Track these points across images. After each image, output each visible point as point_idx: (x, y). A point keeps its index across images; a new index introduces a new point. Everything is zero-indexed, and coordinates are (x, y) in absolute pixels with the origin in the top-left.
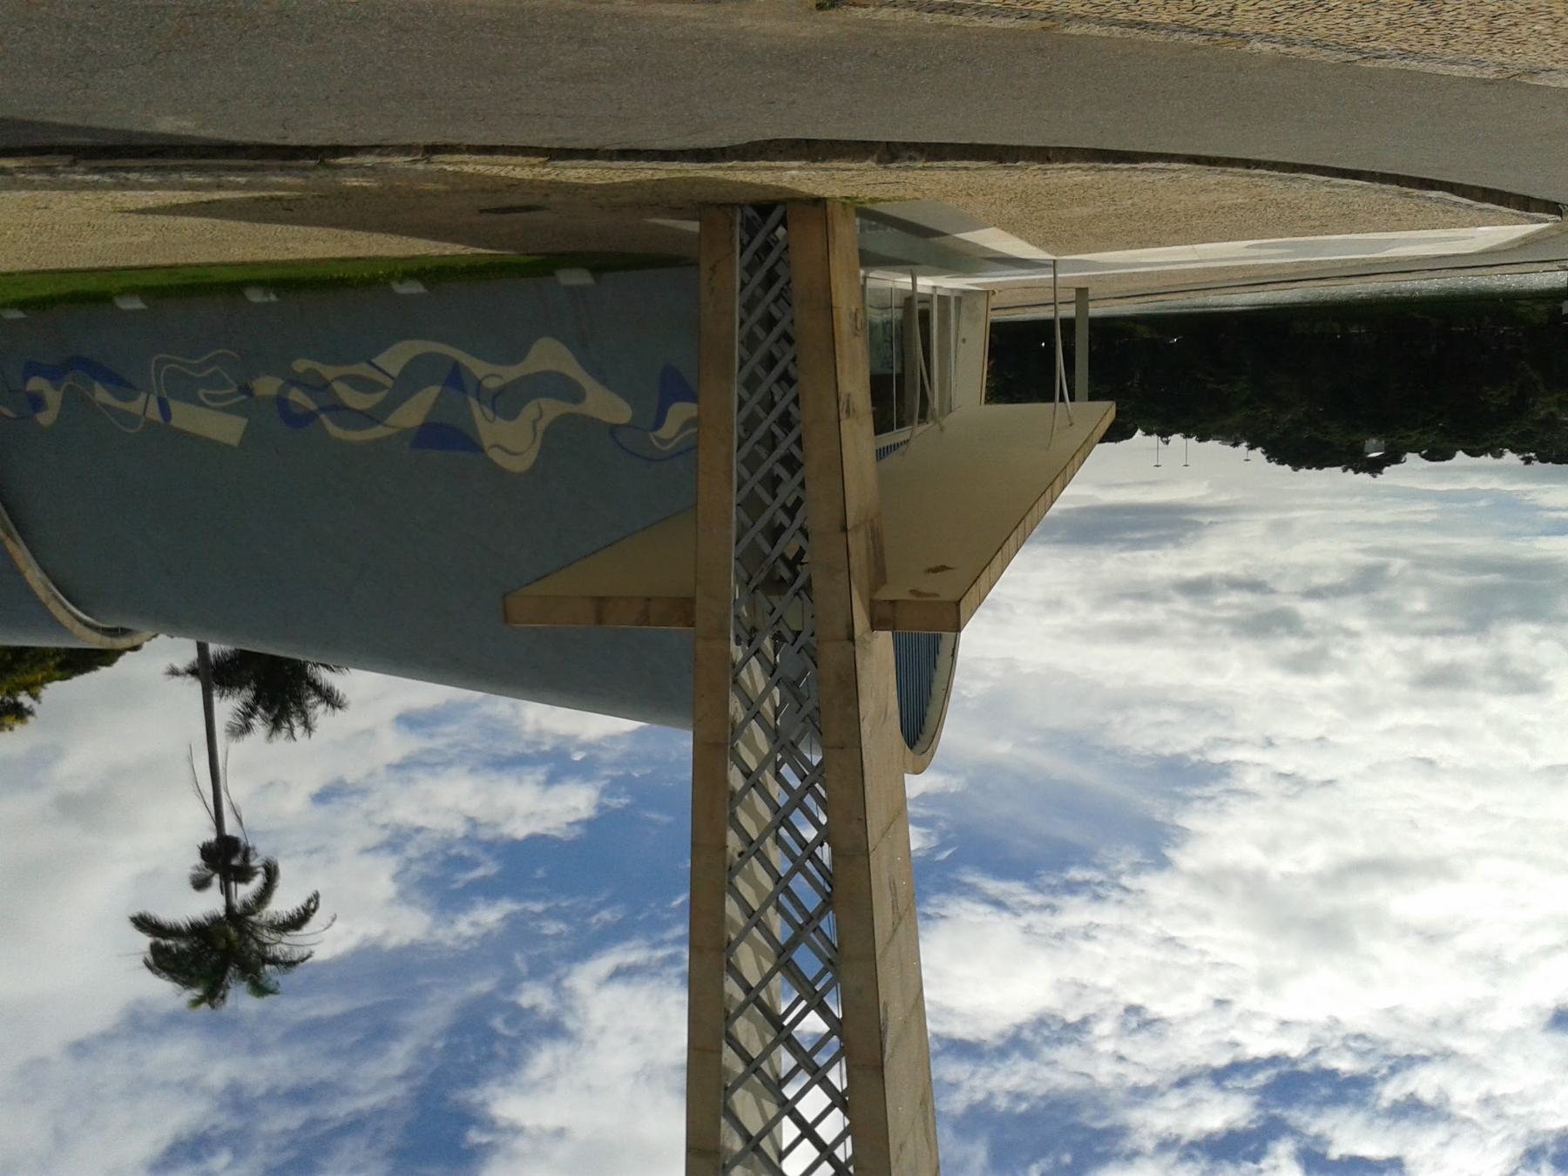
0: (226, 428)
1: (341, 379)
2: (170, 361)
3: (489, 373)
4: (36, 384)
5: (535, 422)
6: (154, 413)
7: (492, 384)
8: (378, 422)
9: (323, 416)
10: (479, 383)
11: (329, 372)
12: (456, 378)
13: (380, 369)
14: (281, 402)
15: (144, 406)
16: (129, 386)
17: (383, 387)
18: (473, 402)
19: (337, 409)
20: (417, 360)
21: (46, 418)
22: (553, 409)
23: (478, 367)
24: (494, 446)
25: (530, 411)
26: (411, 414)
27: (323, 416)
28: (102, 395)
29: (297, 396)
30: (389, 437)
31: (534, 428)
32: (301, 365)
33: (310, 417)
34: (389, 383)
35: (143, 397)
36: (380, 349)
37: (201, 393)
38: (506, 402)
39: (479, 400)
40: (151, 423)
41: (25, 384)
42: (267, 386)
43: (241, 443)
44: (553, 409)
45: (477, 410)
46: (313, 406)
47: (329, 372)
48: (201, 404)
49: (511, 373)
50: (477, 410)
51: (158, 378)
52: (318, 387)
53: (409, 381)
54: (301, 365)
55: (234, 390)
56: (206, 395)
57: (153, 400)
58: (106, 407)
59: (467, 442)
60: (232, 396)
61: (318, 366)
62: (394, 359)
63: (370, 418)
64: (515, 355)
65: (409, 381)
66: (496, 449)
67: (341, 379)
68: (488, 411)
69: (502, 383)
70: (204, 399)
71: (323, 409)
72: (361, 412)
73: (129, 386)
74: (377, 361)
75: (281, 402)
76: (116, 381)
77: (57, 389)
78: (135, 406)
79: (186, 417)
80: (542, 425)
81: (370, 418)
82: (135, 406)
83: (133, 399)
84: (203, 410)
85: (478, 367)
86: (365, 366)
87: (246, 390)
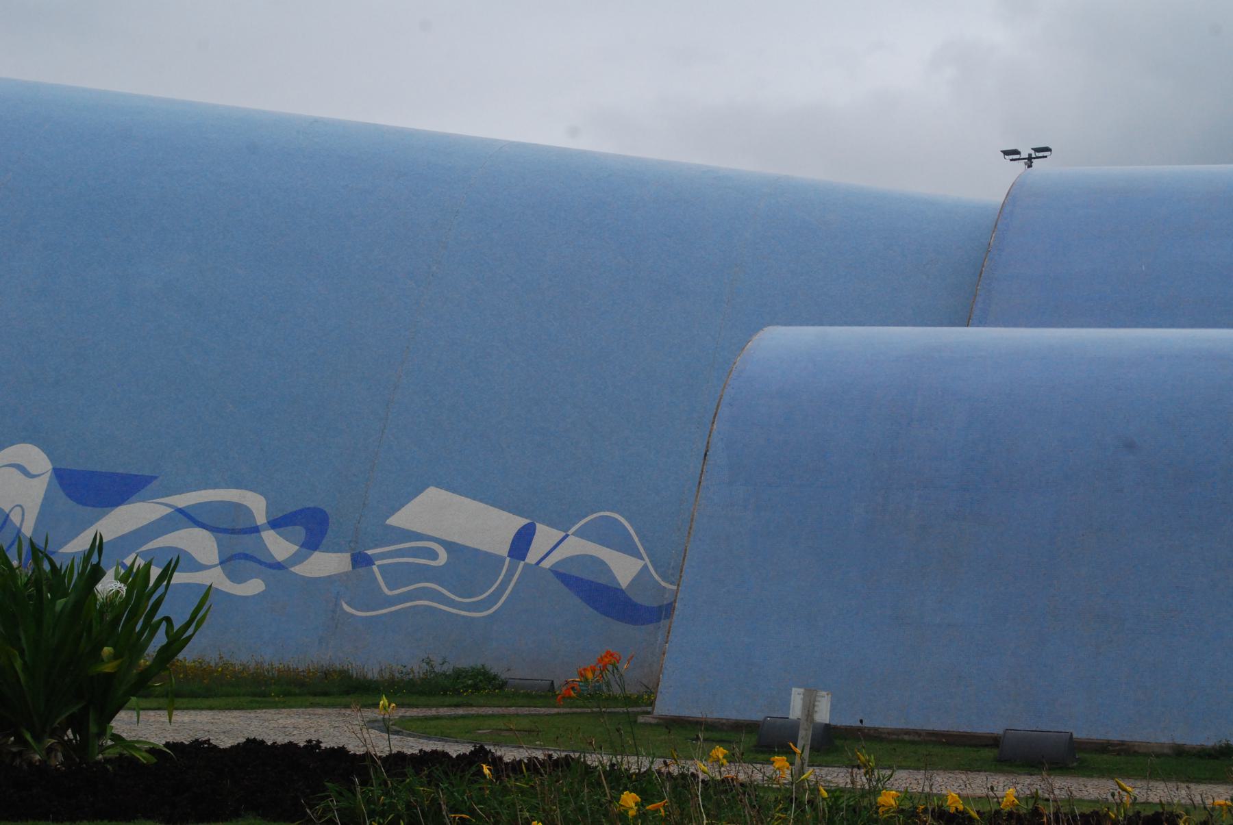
6: (545, 536)
9: (261, 519)
11: (215, 578)
14: (313, 543)
27: (261, 519)
29: (279, 546)
32: (254, 587)
33: (274, 524)
35: (546, 564)
39: (19, 531)
40: (561, 522)
48: (450, 546)
54: (254, 587)
56: (433, 555)
57: (532, 557)
60: (383, 556)
61: (227, 586)
63: (188, 517)
66: (33, 471)
68: (15, 518)
71: (256, 530)
81: (188, 517)
82: (576, 546)
83: (572, 559)
87: (361, 560)
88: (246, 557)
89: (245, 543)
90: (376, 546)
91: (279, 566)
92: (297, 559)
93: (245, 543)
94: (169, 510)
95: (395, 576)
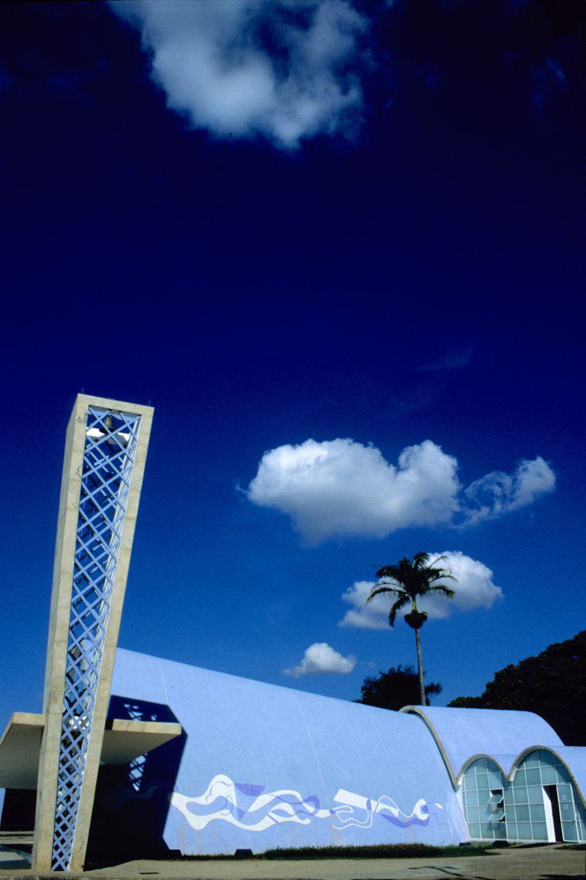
0: (345, 797)
1: (290, 816)
2: (364, 825)
3: (227, 816)
4: (423, 817)
5: (210, 794)
6: (373, 803)
7: (227, 811)
8: (277, 797)
9: (301, 800)
10: (231, 811)
11: (295, 819)
12: (241, 814)
13: (275, 821)
14: (318, 807)
15: (378, 806)
16: (384, 816)
17: (273, 812)
18: (235, 804)
19: (294, 803)
20: (254, 822)
21: (422, 802)
22: (201, 800)
23: (230, 818)
24: (230, 786)
25: (211, 800)
26: (263, 799)
28: (395, 812)
29: (310, 808)
30: (274, 791)
31: (211, 793)
32: (307, 821)
33: (307, 801)
34: (270, 813)
35: (377, 811)
36: (272, 827)
37: (352, 811)
38: (222, 803)
40: (376, 799)
41: (429, 818)
42: (323, 814)
43: (338, 790)
44: (201, 800)
45: (233, 800)
46: (305, 805)
47: (295, 819)
48: (354, 808)
49: (217, 815)
50: (233, 800)
51: (370, 817)
52: (301, 813)
53: (262, 813)
54: (307, 821)
55: (337, 813)
57: (373, 809)
58: (394, 806)
59: (238, 786)
62: (264, 824)
63: (280, 799)
64: (215, 822)
65: (262, 813)
67: (290, 816)
68: (229, 799)
69: (221, 812)
70: (350, 808)
71: (301, 803)
72: (284, 802)
73: (384, 816)
74: (275, 823)
75: (318, 807)
76: (391, 819)
77: (415, 815)
78: (382, 806)
79: (359, 801)
80: (208, 792)
81: (280, 799)
82: (382, 806)
83: (381, 811)
84: (355, 805)
85: (230, 818)
86: (279, 821)
87: (332, 812)
88: (301, 811)
89: (299, 807)
90: (335, 807)
91: (311, 814)
92: (316, 812)
93: (299, 807)
94: (273, 797)
95: (342, 815)
